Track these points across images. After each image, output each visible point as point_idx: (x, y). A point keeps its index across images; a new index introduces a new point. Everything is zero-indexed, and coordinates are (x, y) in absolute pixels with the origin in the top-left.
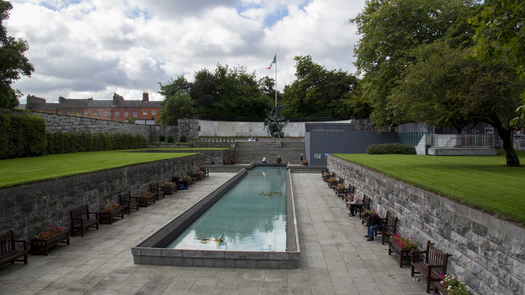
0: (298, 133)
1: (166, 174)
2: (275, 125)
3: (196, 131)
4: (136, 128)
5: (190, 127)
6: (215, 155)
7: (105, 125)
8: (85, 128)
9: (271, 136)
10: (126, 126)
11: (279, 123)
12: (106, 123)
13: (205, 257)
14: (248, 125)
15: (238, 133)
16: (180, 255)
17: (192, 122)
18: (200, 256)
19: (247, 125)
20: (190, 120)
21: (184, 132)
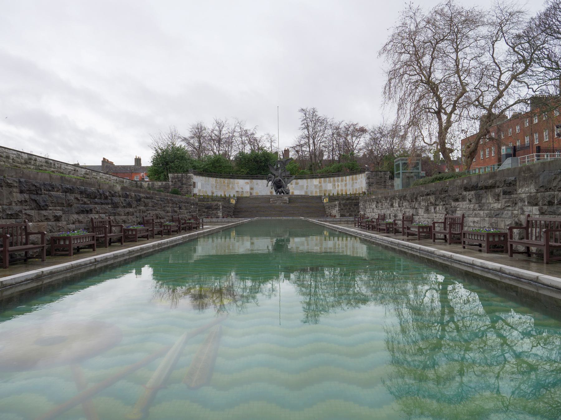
2: (280, 180)
6: (212, 208)
8: (36, 169)
9: (274, 193)
14: (249, 182)
15: (237, 192)
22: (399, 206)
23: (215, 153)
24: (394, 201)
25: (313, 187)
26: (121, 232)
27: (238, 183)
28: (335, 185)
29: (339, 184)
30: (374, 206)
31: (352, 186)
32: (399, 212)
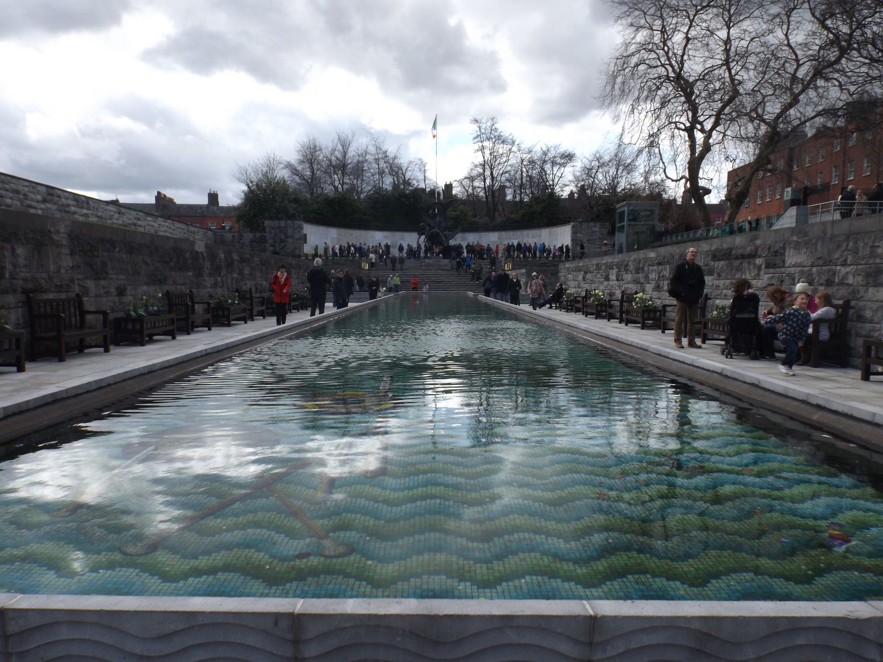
1: (219, 279)
2: (438, 234)
3: (299, 242)
4: (186, 231)
7: (112, 213)
8: (60, 211)
10: (162, 223)
12: (115, 210)
20: (288, 222)
21: (277, 244)
22: (618, 280)
23: (336, 188)
26: (209, 313)
30: (580, 277)
32: (617, 288)
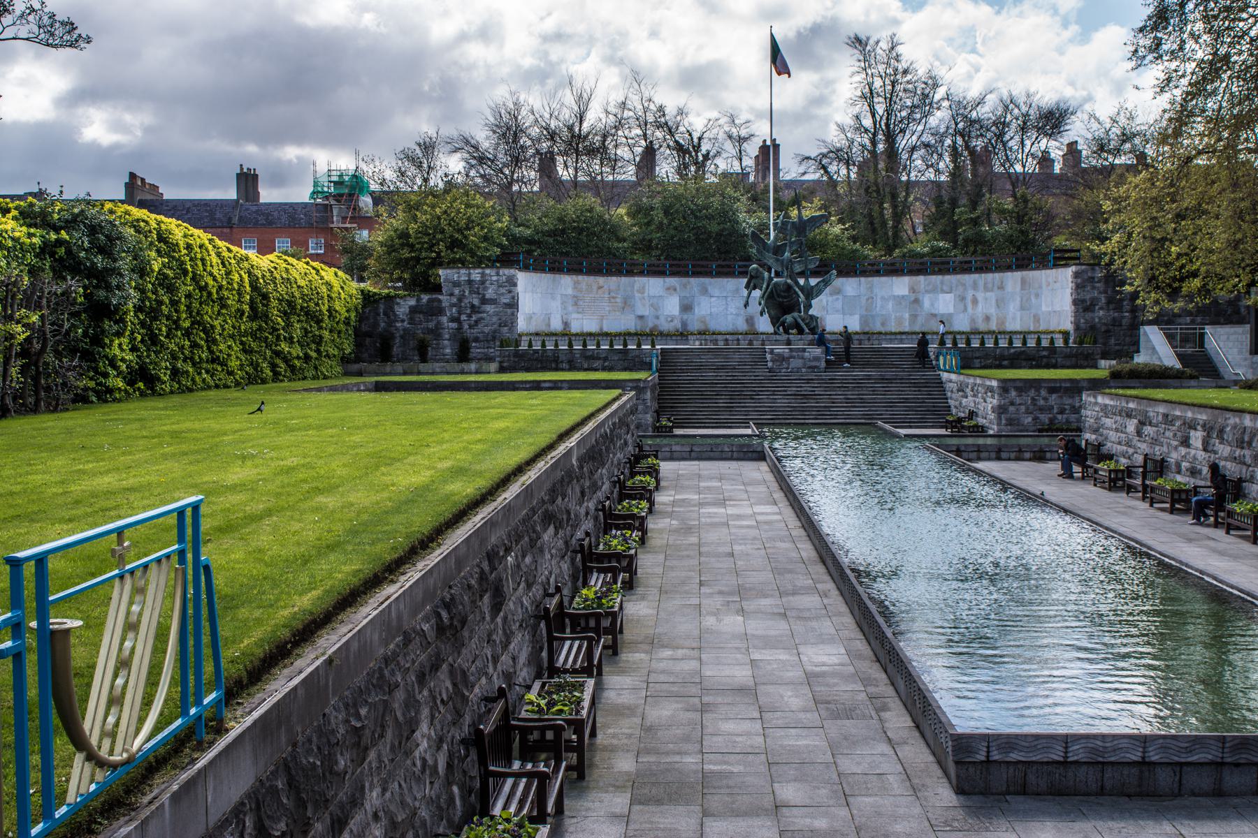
0: (857, 317)
2: (789, 287)
5: (487, 296)
11: (802, 281)
13: (1229, 760)
15: (641, 317)
16: (1135, 756)
17: (495, 278)
18: (1210, 757)
19: (675, 290)
20: (488, 271)
24: (1192, 433)
25: (890, 305)
27: (642, 291)
28: (963, 299)
29: (980, 296)
31: (1022, 308)
